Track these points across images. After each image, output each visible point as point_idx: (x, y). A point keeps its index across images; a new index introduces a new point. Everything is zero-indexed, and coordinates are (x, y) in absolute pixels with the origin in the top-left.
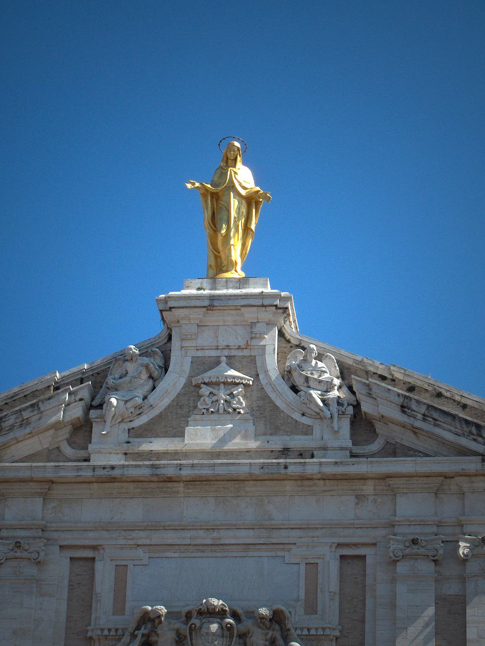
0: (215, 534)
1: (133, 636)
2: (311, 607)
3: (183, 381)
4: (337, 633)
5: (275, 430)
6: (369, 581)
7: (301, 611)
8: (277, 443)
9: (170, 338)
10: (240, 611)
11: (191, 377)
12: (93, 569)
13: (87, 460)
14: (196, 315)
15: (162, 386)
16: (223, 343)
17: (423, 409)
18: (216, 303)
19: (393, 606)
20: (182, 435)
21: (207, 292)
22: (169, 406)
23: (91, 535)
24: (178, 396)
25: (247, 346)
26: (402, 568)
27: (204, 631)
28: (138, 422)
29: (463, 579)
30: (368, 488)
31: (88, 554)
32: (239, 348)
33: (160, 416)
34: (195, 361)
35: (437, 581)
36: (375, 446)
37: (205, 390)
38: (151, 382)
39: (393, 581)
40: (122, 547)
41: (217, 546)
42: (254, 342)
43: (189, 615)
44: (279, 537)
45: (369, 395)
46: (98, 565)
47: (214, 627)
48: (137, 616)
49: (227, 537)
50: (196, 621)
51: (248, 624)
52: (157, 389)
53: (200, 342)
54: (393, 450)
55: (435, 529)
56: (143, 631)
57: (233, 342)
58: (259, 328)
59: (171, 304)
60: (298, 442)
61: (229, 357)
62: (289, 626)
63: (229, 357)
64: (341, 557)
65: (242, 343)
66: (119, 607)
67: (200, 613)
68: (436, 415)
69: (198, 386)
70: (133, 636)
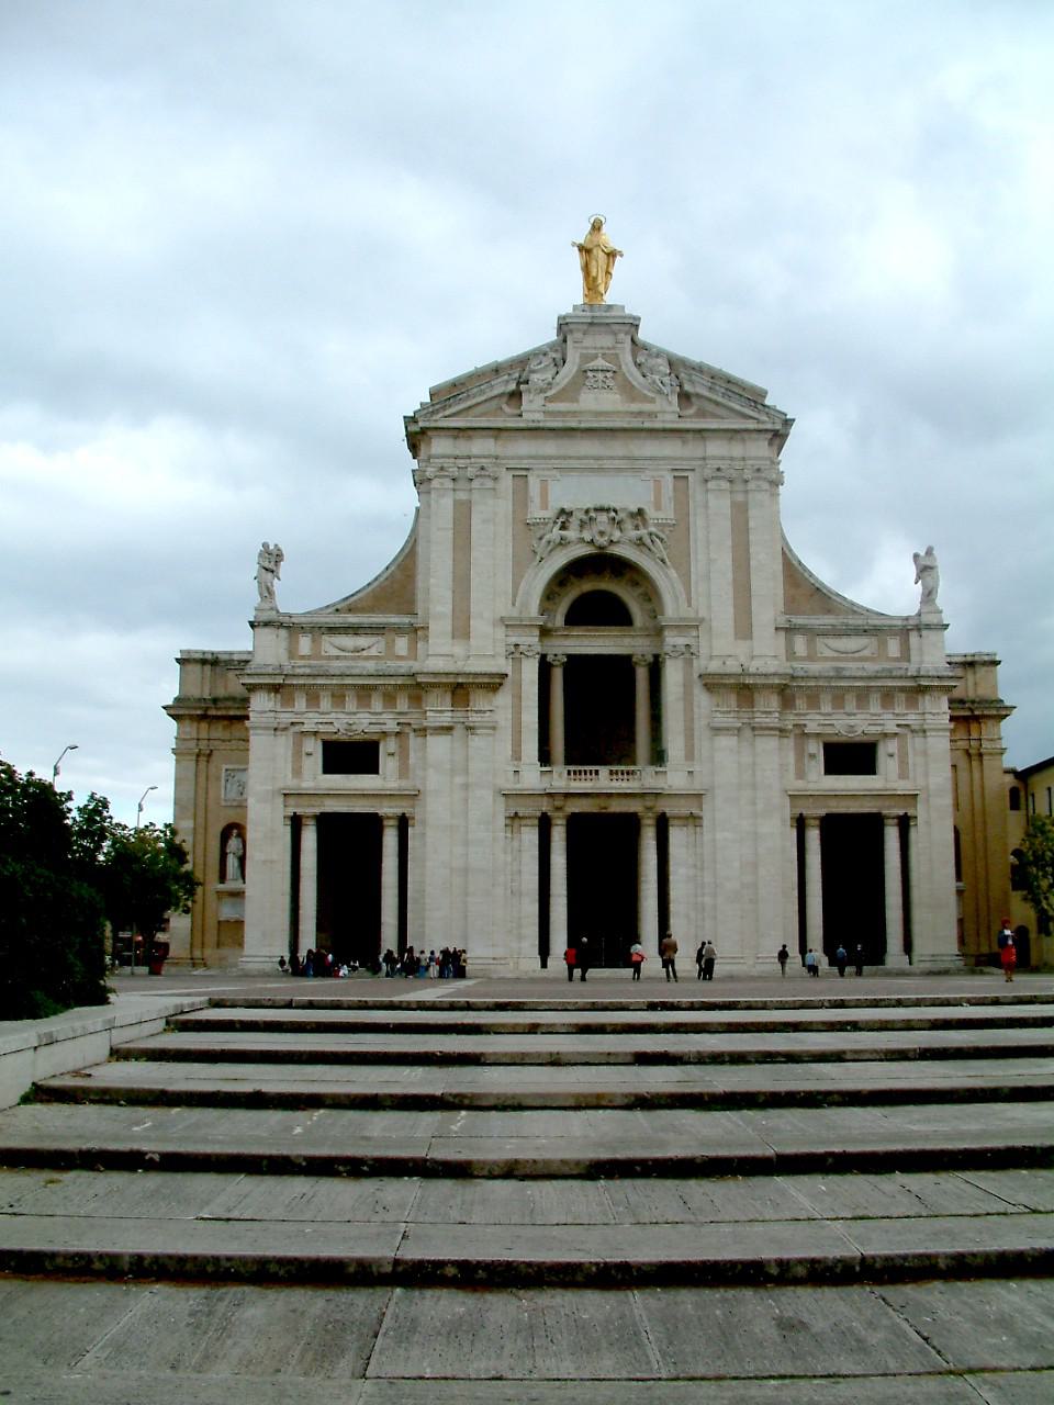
0: (600, 462)
1: (555, 523)
2: (658, 507)
3: (575, 369)
4: (674, 522)
5: (633, 400)
6: (690, 492)
7: (653, 510)
8: (635, 407)
9: (565, 341)
10: (618, 508)
11: (580, 366)
12: (527, 482)
13: (521, 415)
14: (585, 327)
15: (564, 371)
16: (599, 345)
17: (723, 390)
18: (596, 321)
19: (706, 507)
20: (577, 401)
21: (588, 314)
22: (568, 383)
23: (526, 461)
24: (573, 378)
25: (614, 348)
26: (711, 485)
27: (598, 520)
28: (549, 394)
29: (746, 492)
30: (690, 436)
31: (524, 473)
32: (609, 348)
33: (563, 389)
34: (582, 356)
35: (731, 492)
36: (691, 411)
37: (590, 374)
38: (554, 370)
39: (707, 491)
40: (543, 469)
41: (601, 469)
42: (619, 345)
43: (587, 511)
44: (638, 464)
45: (690, 381)
46: (531, 479)
47: (603, 517)
48: (556, 511)
49: (607, 464)
50: (593, 514)
51: (622, 515)
52: (561, 373)
53: (584, 345)
54: (702, 414)
55: (729, 462)
56: (562, 520)
57: (605, 345)
58: (621, 336)
59: (568, 320)
60: (647, 407)
61: (603, 354)
62: (647, 517)
63: (603, 354)
64: (675, 477)
65: (610, 346)
66: (545, 506)
67: (596, 510)
68: (730, 393)
69: (585, 371)
70: (555, 523)
